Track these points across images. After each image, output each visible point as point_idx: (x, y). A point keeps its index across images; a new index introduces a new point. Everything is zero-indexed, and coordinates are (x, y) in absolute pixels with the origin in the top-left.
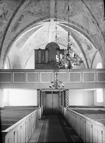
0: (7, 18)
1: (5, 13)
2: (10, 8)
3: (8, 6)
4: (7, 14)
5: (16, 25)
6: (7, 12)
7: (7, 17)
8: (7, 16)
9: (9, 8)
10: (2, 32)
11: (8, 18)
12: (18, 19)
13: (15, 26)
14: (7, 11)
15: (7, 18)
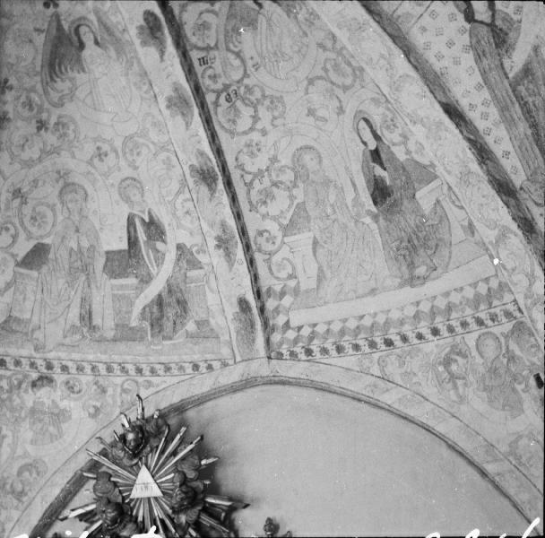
0: (408, 152)
1: (372, 145)
2: (348, 81)
3: (332, 94)
4: (389, 137)
5: (517, 110)
6: (366, 121)
7: (400, 154)
8: (394, 149)
9: (345, 88)
10: (487, 280)
11: (412, 146)
12: (479, 57)
13: (523, 128)
14: (363, 124)
15: (408, 152)
